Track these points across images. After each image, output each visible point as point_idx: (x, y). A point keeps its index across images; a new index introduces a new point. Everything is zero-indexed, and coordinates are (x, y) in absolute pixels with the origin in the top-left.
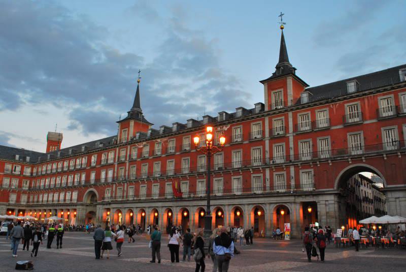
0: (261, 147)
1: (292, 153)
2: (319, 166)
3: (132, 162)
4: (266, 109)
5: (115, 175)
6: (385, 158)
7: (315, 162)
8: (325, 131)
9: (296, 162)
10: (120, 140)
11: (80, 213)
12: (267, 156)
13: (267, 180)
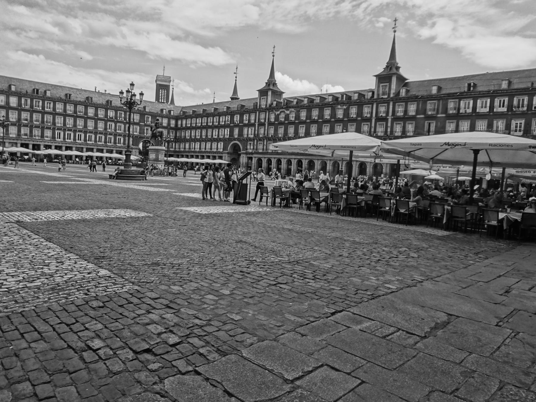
0: (369, 123)
1: (389, 130)
3: (270, 124)
4: (375, 97)
5: (256, 133)
8: (413, 118)
10: (260, 105)
12: (373, 130)
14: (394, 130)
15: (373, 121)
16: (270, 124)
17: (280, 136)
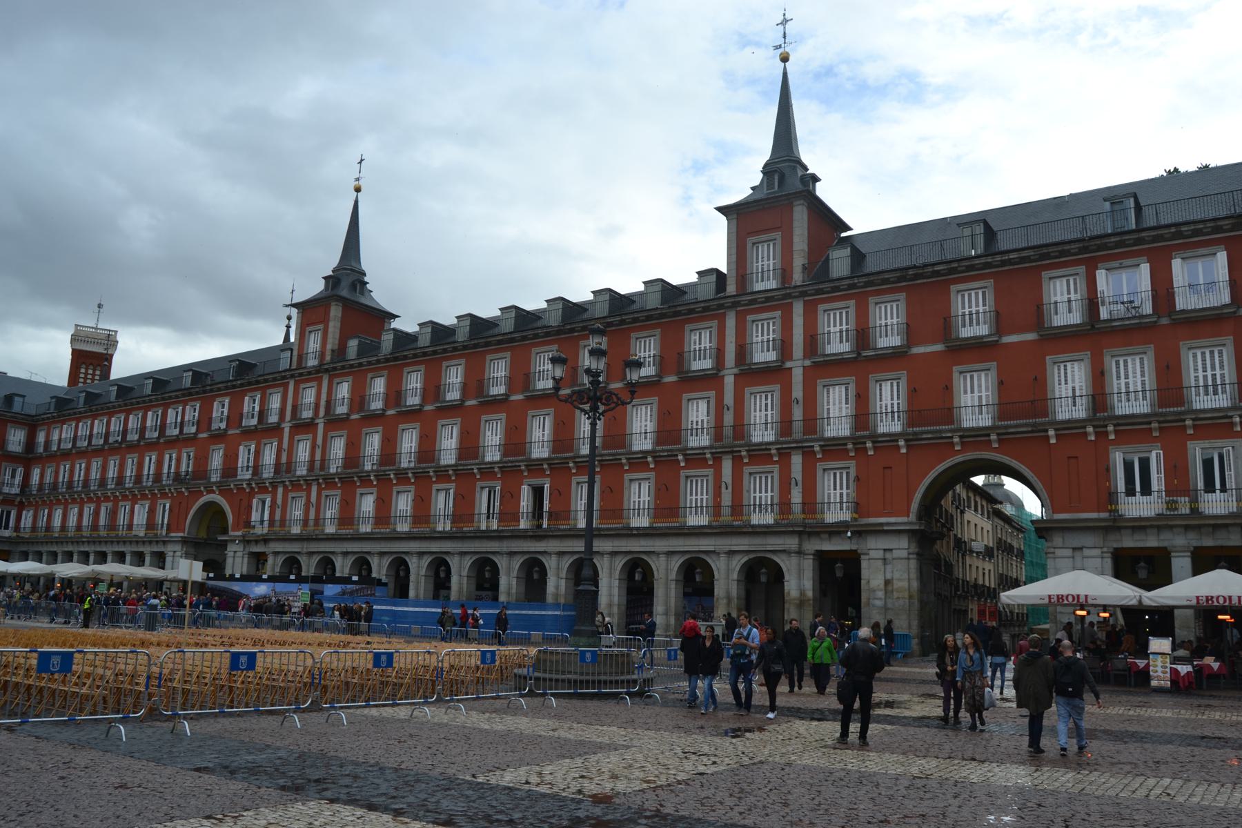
1: (798, 413)
3: (335, 423)
4: (731, 289)
5: (284, 459)
6: (1053, 441)
7: (862, 443)
9: (807, 441)
14: (822, 412)
15: (729, 381)
16: (335, 423)
17: (368, 467)
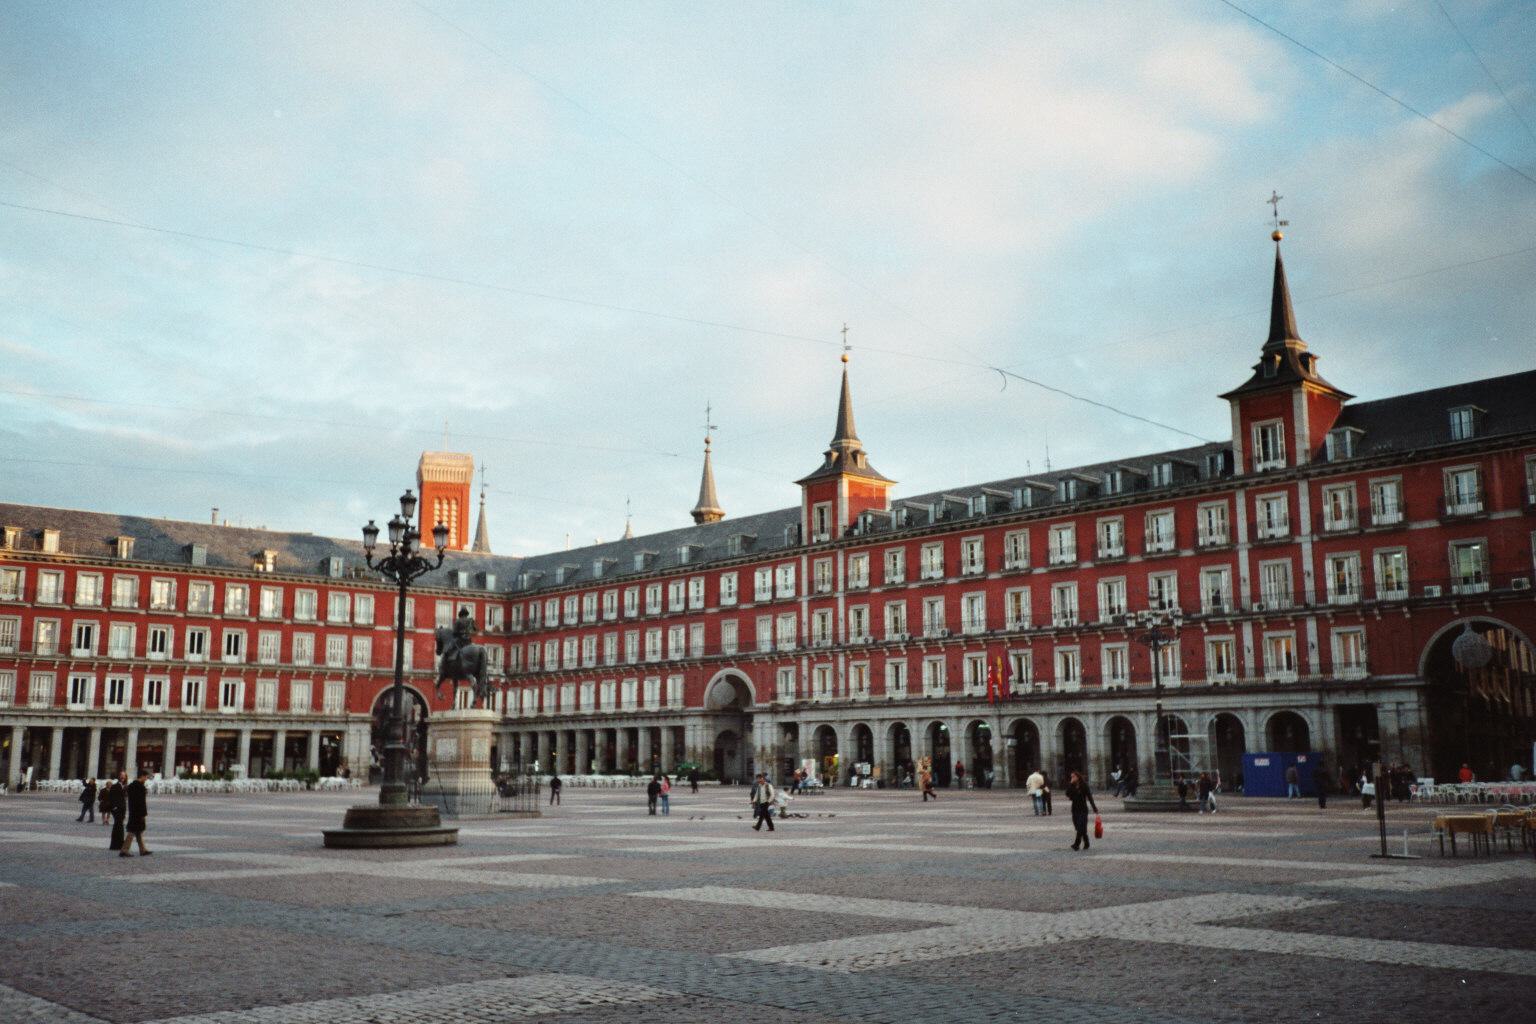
1: (1310, 585)
2: (1378, 618)
3: (854, 597)
4: (1239, 470)
7: (1366, 611)
8: (1392, 536)
11: (699, 740)
12: (1246, 590)
13: (1246, 651)
15: (1243, 557)
16: (854, 597)
